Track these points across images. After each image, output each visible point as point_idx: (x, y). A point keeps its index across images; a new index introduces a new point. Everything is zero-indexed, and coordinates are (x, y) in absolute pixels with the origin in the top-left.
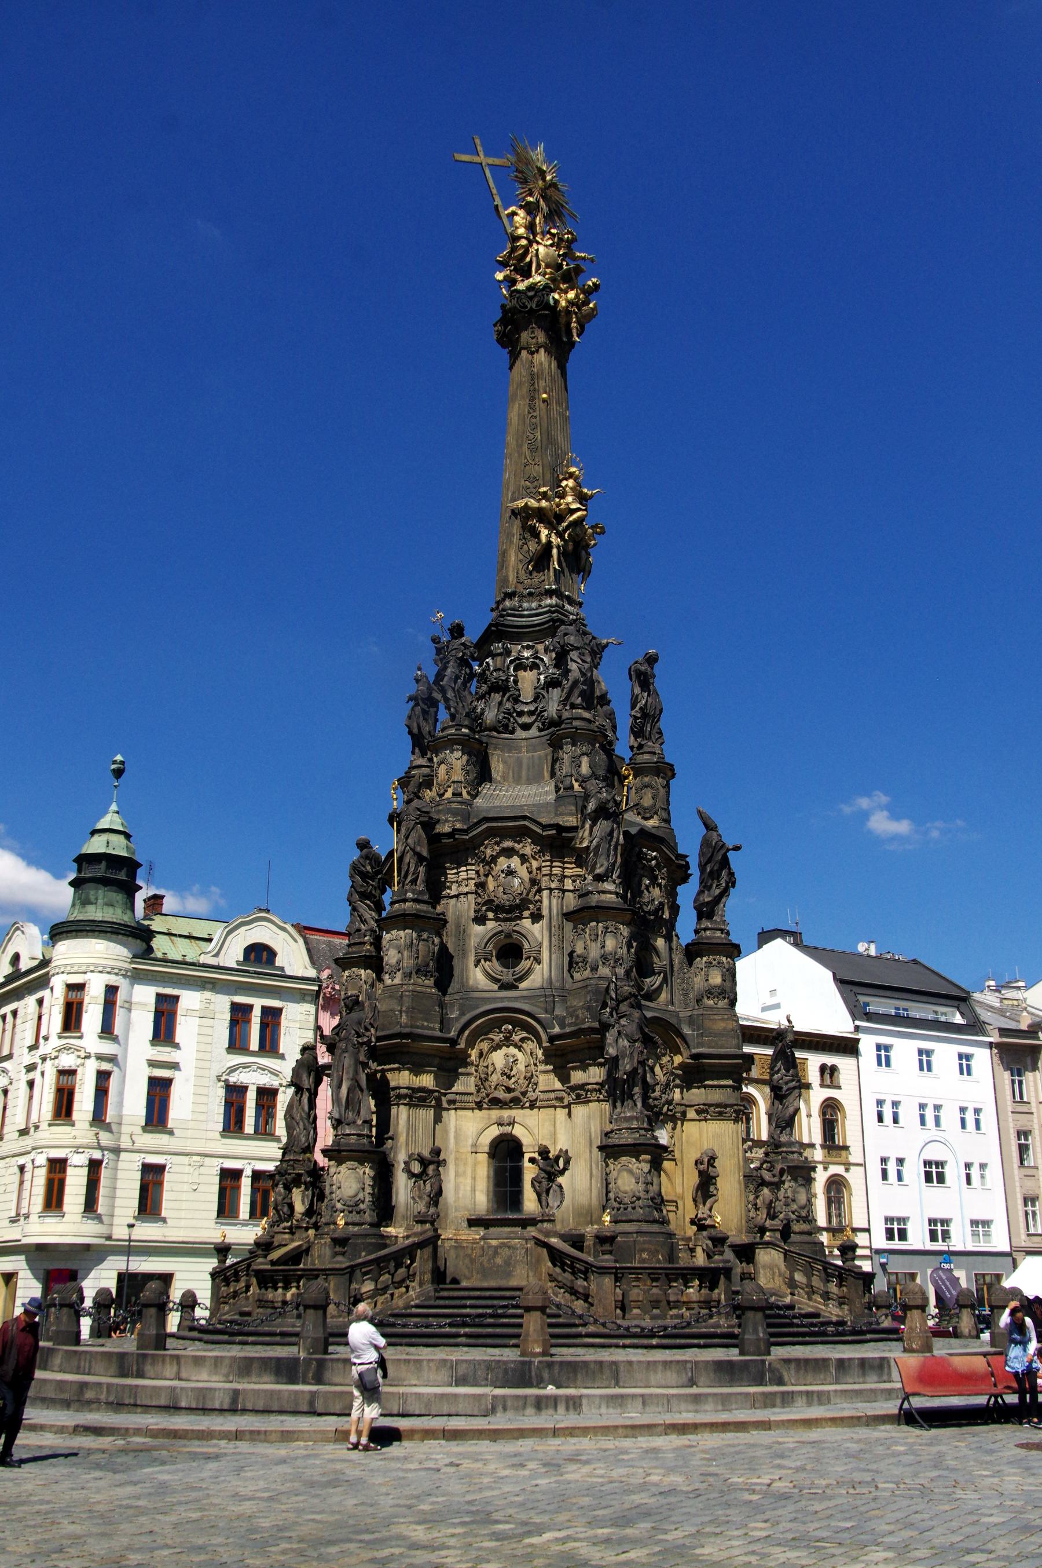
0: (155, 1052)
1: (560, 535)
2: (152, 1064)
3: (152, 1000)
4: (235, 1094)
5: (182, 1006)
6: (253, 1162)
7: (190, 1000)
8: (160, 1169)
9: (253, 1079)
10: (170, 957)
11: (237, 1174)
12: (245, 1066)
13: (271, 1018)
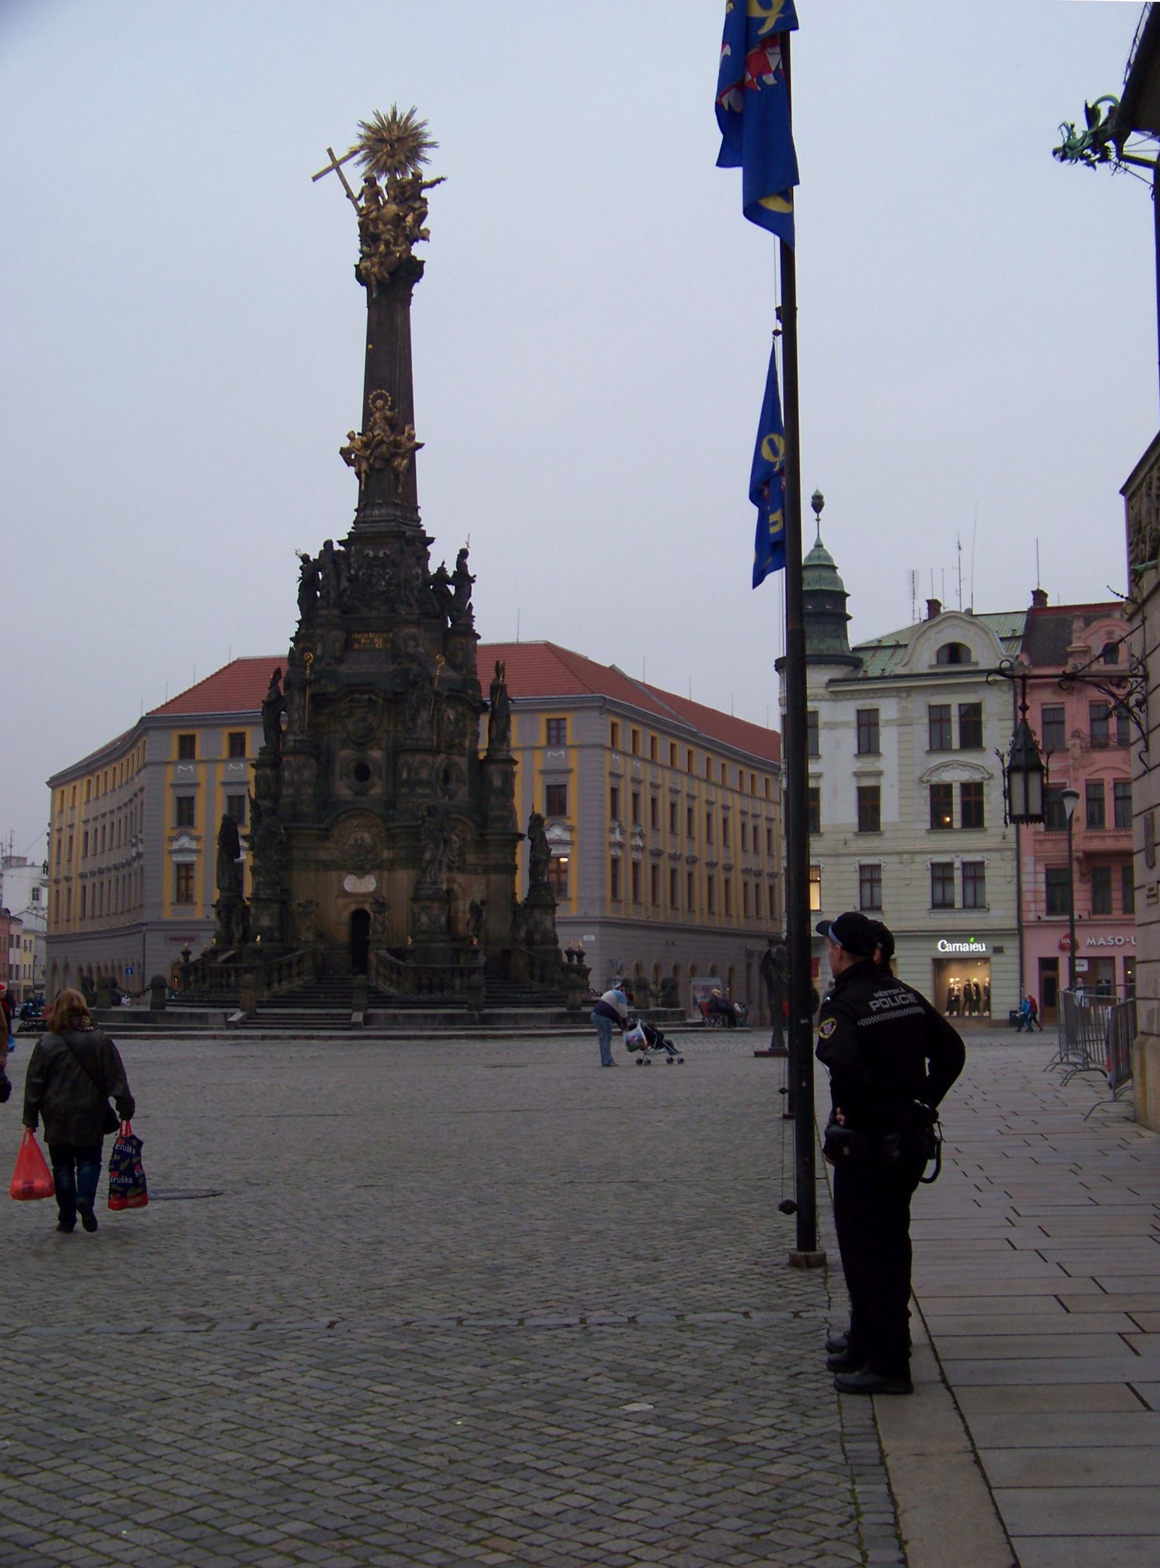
0: (859, 765)
1: (368, 459)
2: (858, 775)
3: (852, 717)
4: (940, 795)
5: (883, 716)
6: (961, 855)
7: (888, 709)
8: (877, 868)
9: (956, 776)
10: (870, 675)
11: (950, 865)
12: (945, 765)
13: (972, 718)
